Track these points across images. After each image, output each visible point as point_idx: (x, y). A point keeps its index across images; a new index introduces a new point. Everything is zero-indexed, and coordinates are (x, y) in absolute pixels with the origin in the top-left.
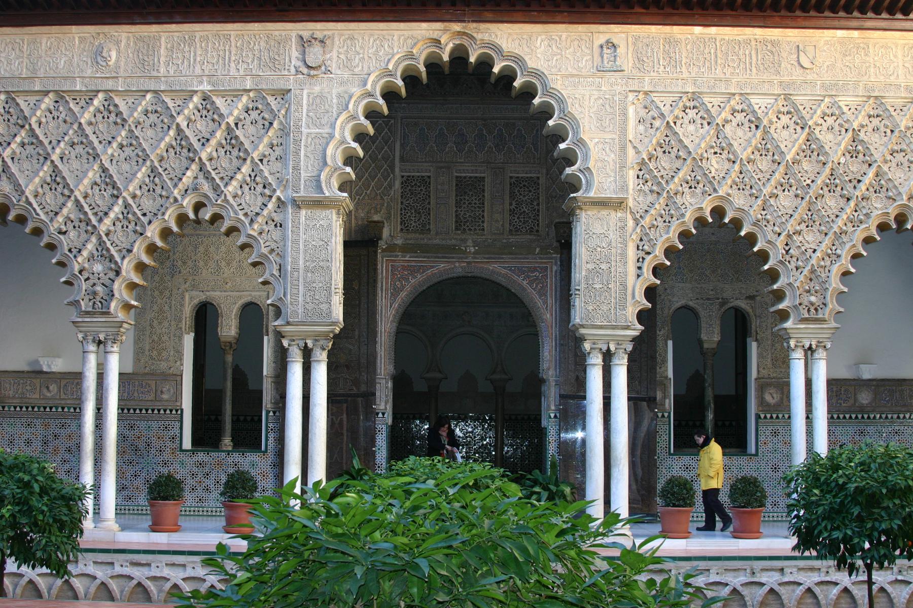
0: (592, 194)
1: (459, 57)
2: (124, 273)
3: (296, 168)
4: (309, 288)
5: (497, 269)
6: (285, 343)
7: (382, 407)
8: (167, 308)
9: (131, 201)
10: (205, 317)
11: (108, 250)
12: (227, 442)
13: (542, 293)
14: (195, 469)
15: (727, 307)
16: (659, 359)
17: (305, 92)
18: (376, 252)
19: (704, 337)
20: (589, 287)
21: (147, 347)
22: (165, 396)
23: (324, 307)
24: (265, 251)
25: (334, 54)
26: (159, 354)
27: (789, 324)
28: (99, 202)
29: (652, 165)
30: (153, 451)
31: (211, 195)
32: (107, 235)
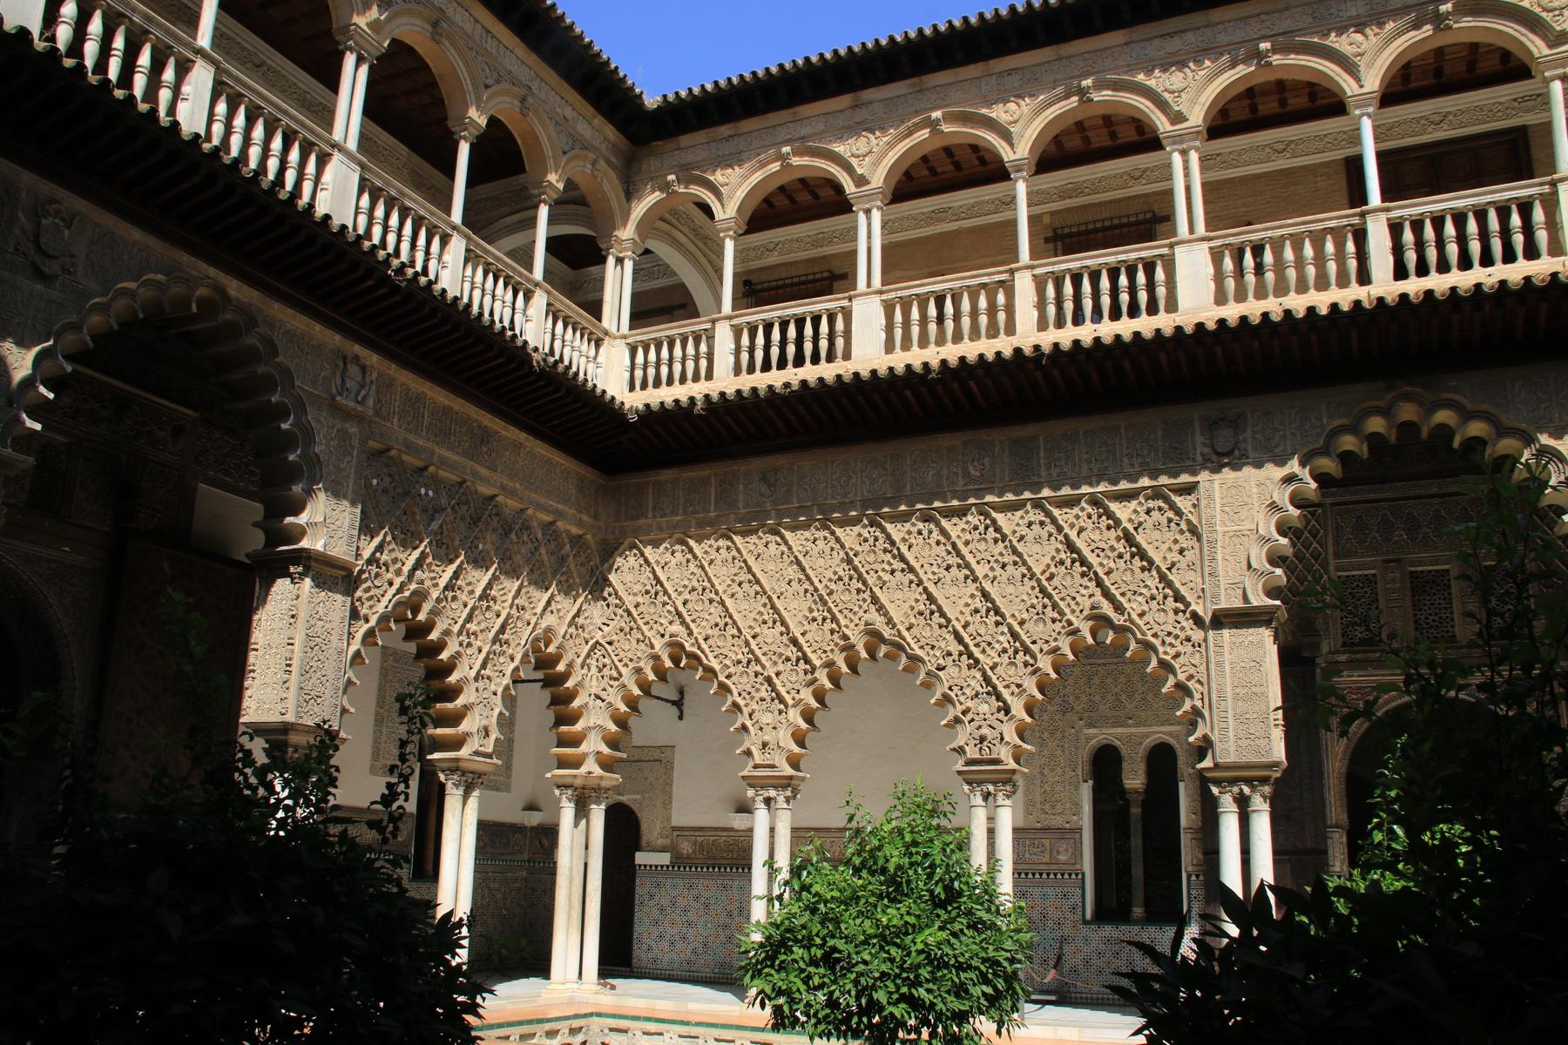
2: (1013, 712)
4: (1241, 719)
6: (1215, 790)
7: (1337, 869)
8: (1059, 752)
9: (1017, 628)
10: (1105, 763)
11: (994, 687)
17: (1216, 484)
18: (1313, 673)
21: (1039, 799)
22: (1062, 858)
23: (1262, 742)
24: (1182, 677)
25: (1249, 434)
26: (1053, 807)
28: (982, 632)
30: (1050, 924)
32: (992, 668)
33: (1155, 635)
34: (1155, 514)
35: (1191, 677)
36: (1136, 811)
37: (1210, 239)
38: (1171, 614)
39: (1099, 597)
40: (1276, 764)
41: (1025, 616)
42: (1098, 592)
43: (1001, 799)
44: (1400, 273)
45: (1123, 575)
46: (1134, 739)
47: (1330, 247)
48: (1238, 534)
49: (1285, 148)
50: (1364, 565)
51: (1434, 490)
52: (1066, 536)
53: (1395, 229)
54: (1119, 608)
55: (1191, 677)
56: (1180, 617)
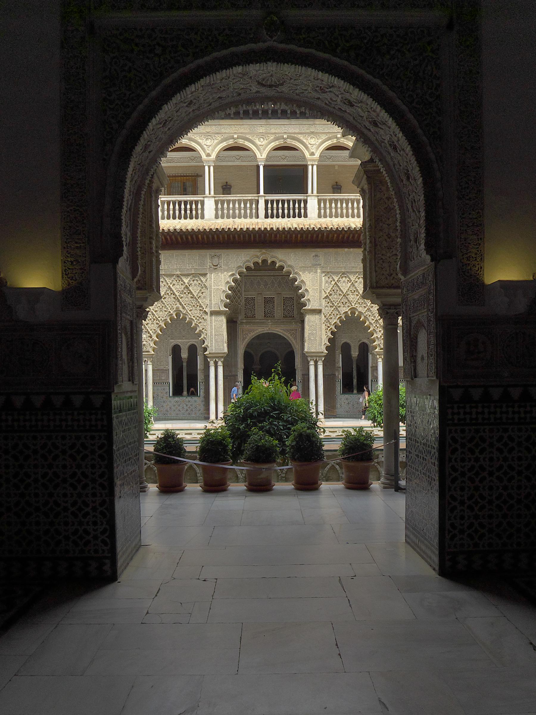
0: (309, 308)
1: (264, 261)
3: (210, 300)
5: (279, 330)
9: (154, 313)
10: (176, 350)
11: (147, 330)
12: (185, 393)
13: (295, 338)
14: (175, 404)
15: (361, 342)
16: (336, 361)
19: (352, 353)
20: (309, 339)
22: (163, 378)
24: (201, 329)
27: (377, 350)
29: (330, 297)
31: (182, 310)
33: (194, 317)
34: (195, 281)
35: (203, 329)
36: (185, 364)
37: (215, 197)
38: (199, 311)
39: (178, 305)
40: (225, 353)
41: (157, 309)
42: (178, 303)
43: (149, 363)
44: (266, 217)
45: (186, 299)
46: (184, 344)
47: (248, 205)
48: (218, 289)
49: (239, 158)
50: (252, 294)
51: (272, 274)
52: (169, 286)
53: (266, 202)
54: (184, 308)
55: (203, 329)
56: (201, 312)
